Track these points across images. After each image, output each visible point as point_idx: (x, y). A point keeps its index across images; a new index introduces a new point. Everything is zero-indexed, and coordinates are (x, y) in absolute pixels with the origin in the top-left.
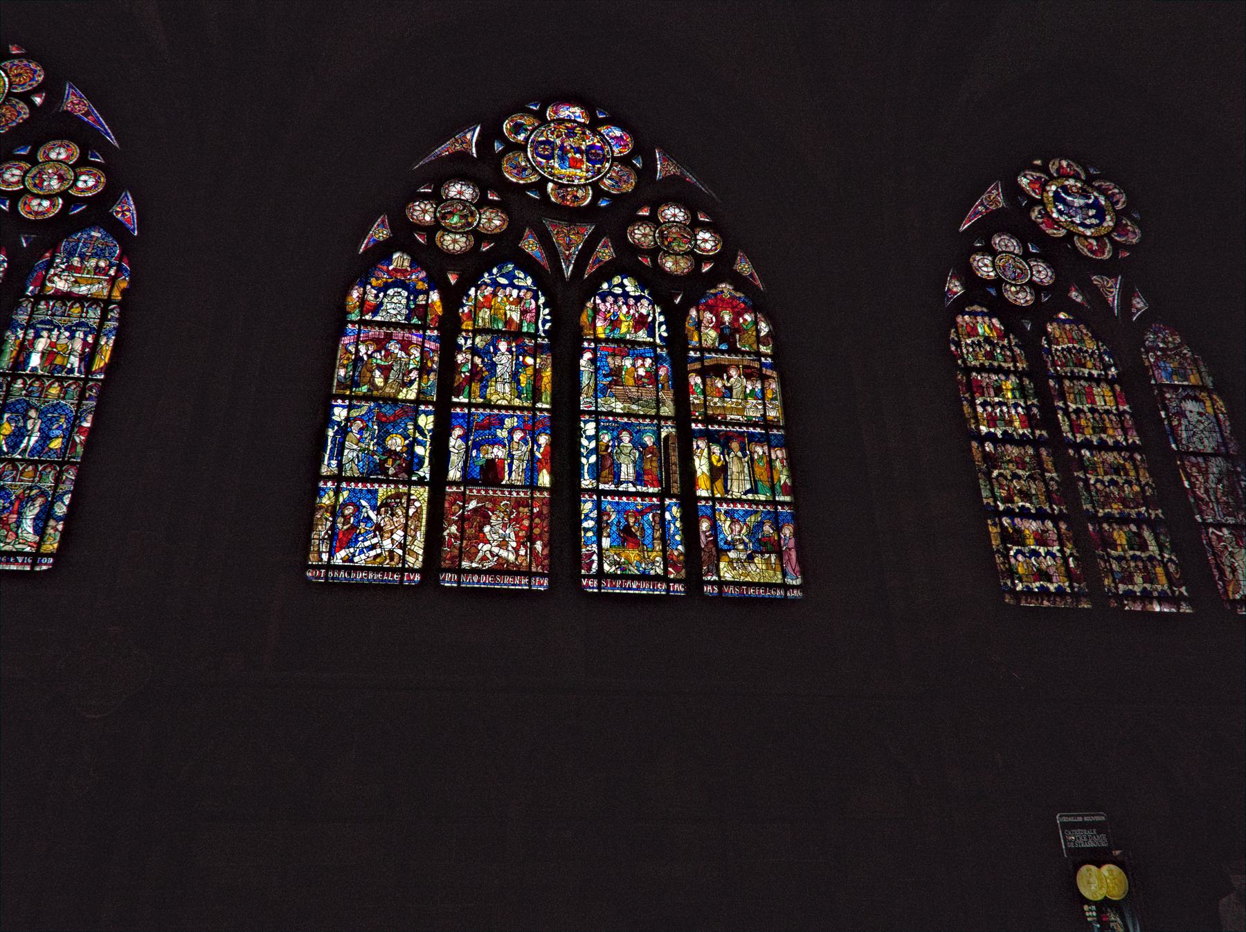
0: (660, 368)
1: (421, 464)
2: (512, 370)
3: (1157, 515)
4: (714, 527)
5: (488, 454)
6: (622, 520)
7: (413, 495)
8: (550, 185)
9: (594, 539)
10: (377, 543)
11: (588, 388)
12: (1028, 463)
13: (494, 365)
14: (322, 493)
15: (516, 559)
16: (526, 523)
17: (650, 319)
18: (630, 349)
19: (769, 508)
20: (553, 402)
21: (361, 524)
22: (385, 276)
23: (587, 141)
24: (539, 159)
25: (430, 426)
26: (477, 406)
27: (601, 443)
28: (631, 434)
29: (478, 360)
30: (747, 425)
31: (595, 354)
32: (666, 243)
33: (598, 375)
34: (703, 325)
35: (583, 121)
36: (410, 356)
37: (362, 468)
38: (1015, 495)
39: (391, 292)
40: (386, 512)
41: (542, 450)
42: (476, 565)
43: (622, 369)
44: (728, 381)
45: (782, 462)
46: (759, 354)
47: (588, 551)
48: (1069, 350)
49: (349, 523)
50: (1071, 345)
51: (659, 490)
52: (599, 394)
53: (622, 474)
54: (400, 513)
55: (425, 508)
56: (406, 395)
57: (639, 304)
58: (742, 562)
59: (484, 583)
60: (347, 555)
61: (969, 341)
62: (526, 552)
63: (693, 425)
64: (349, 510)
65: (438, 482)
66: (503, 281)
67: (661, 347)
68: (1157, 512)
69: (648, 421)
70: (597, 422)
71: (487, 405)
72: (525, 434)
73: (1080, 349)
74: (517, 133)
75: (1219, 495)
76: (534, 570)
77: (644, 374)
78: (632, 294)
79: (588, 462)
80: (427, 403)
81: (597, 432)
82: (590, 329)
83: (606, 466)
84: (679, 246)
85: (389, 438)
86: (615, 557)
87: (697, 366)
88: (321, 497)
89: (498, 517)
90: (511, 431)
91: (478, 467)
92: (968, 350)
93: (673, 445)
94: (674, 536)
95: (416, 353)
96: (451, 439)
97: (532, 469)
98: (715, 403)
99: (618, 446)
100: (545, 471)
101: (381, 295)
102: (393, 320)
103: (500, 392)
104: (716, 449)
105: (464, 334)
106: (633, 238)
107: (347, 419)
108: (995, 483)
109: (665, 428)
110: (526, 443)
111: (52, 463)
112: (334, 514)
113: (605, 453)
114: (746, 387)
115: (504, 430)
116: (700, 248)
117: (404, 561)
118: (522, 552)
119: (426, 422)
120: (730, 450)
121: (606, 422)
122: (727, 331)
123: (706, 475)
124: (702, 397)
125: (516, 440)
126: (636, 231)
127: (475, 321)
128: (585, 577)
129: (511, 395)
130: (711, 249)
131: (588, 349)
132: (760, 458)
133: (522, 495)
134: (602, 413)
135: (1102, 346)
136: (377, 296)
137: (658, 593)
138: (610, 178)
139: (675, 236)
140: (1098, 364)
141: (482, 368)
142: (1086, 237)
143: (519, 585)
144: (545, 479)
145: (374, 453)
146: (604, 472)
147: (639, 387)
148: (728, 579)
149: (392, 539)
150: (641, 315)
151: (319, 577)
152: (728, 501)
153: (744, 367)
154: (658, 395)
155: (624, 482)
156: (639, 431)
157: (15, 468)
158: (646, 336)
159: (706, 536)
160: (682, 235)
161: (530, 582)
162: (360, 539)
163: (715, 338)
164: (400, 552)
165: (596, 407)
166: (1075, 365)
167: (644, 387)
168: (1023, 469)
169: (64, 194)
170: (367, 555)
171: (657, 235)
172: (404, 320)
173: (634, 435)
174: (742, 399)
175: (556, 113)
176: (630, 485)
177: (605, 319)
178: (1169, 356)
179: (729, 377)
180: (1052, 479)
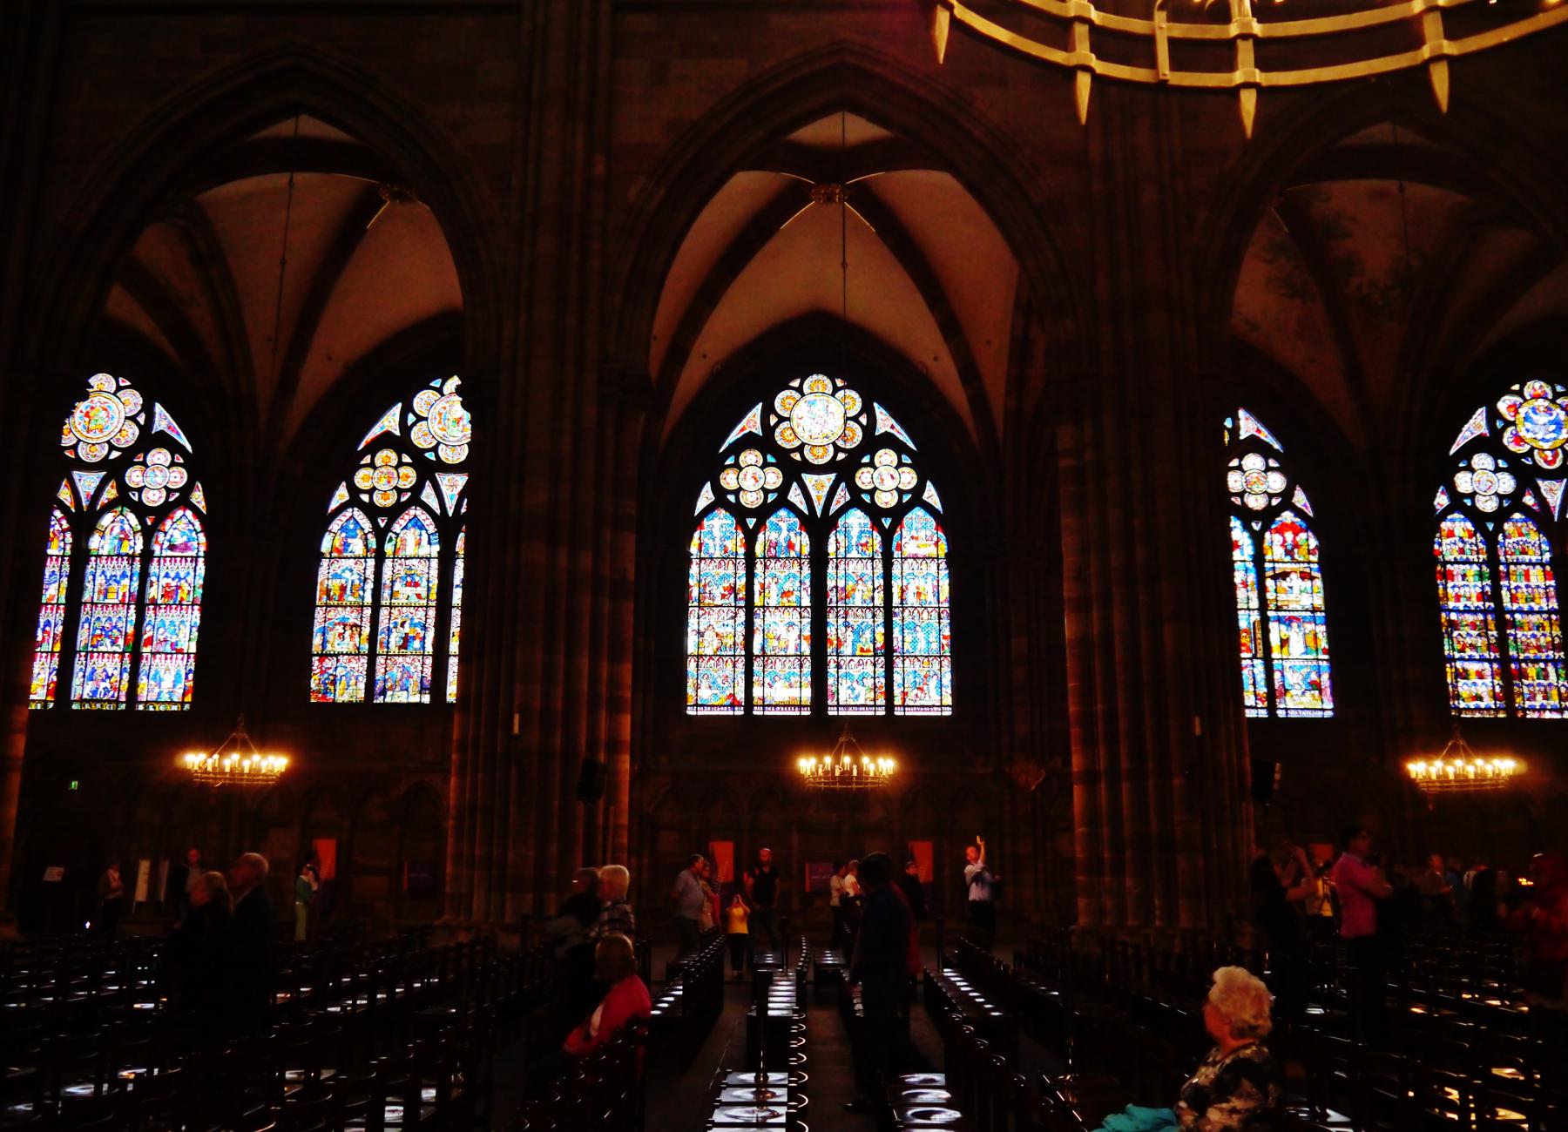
3: (1560, 656)
4: (1283, 676)
48: (1518, 543)
50: (1519, 539)
87: (1271, 573)
93: (1258, 626)
104: (1283, 627)
111: (935, 656)
122: (1289, 547)
139: (1255, 480)
142: (1543, 450)
153: (1301, 572)
157: (919, 661)
169: (897, 489)
180: (1493, 636)
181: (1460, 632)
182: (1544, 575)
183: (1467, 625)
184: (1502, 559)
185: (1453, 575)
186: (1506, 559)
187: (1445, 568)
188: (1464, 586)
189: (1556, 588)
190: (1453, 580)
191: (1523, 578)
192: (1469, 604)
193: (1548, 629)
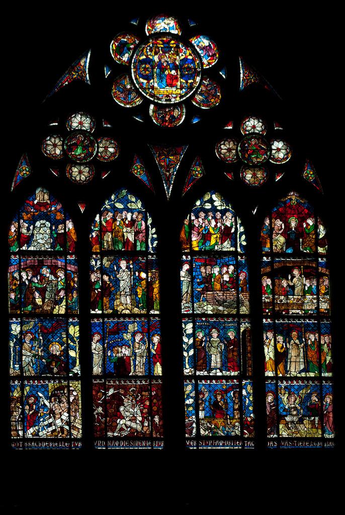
0: (241, 273)
1: (74, 365)
2: (131, 285)
4: (277, 399)
5: (118, 353)
6: (213, 397)
7: (71, 387)
8: (152, 107)
9: (194, 412)
10: (52, 422)
11: (187, 295)
13: (117, 282)
14: (13, 389)
15: (142, 429)
16: (147, 403)
17: (233, 230)
18: (217, 259)
19: (316, 382)
20: (160, 310)
21: (41, 409)
22: (32, 210)
23: (181, 54)
24: (141, 80)
25: (77, 335)
26: (109, 316)
27: (197, 339)
28: (219, 331)
29: (106, 278)
30: (304, 318)
31: (191, 266)
32: (247, 156)
33: (194, 284)
34: (274, 232)
35: (175, 32)
36: (58, 278)
37: (36, 369)
39: (38, 224)
40: (55, 400)
41: (156, 347)
42: (117, 434)
43: (212, 277)
44: (292, 280)
45: (328, 346)
46: (317, 255)
47: (190, 421)
49: (33, 409)
51: (238, 373)
52: (195, 300)
53: (212, 362)
54: (65, 401)
55: (80, 396)
56: (59, 310)
57: (224, 217)
58: (295, 424)
59: (123, 446)
60: (34, 431)
62: (149, 424)
63: (264, 320)
64: (31, 401)
65: (86, 375)
66: (119, 206)
67: (241, 255)
69: (230, 320)
70: (194, 323)
71: (116, 314)
72: (143, 336)
74: (122, 54)
76: (154, 436)
77: (228, 280)
78: (219, 208)
79: (188, 354)
80: (73, 317)
81: (194, 331)
82: (187, 244)
83: (201, 359)
84: (257, 158)
85: (51, 345)
86: (208, 424)
87: (268, 270)
88: (13, 392)
89: (129, 399)
90: (134, 334)
91: (113, 364)
94: (248, 406)
95: (61, 274)
96: (93, 344)
97: (150, 365)
98: (281, 301)
99: (209, 341)
100: (158, 363)
101: (31, 228)
102: (43, 249)
103: (124, 303)
104: (280, 338)
105: (94, 256)
106: (220, 153)
107: (21, 331)
109: (243, 324)
110: (144, 343)
112: (22, 404)
113: (200, 347)
114: (305, 285)
115: (128, 334)
116: (273, 159)
117: (69, 432)
118: (146, 424)
119: (74, 331)
120: (291, 339)
121: (201, 322)
122: (292, 237)
123: (272, 360)
124: (271, 296)
125: (137, 341)
126: (222, 146)
127: (101, 244)
128: (188, 439)
129: (132, 305)
130: (283, 158)
131: (186, 262)
132: (313, 343)
133: (144, 383)
134: (198, 315)
136: (28, 229)
137: (237, 448)
138: (201, 94)
141: (109, 284)
143: (145, 447)
144: (158, 370)
145: (42, 357)
146: (200, 362)
147: (224, 291)
148: (284, 436)
149: (62, 420)
150: (226, 227)
151: (19, 447)
152: (287, 379)
153: (305, 268)
154: (238, 297)
155: (214, 369)
156: (224, 327)
158: (229, 246)
159: (271, 406)
160: (260, 147)
161: (152, 444)
162: (41, 420)
163: (284, 243)
164: (67, 427)
165: (193, 310)
167: (228, 290)
170: (47, 430)
171: (239, 148)
172: (51, 248)
173: (221, 331)
174: (301, 296)
175: (153, 27)
176: (218, 371)
177: (199, 234)
179: (293, 277)
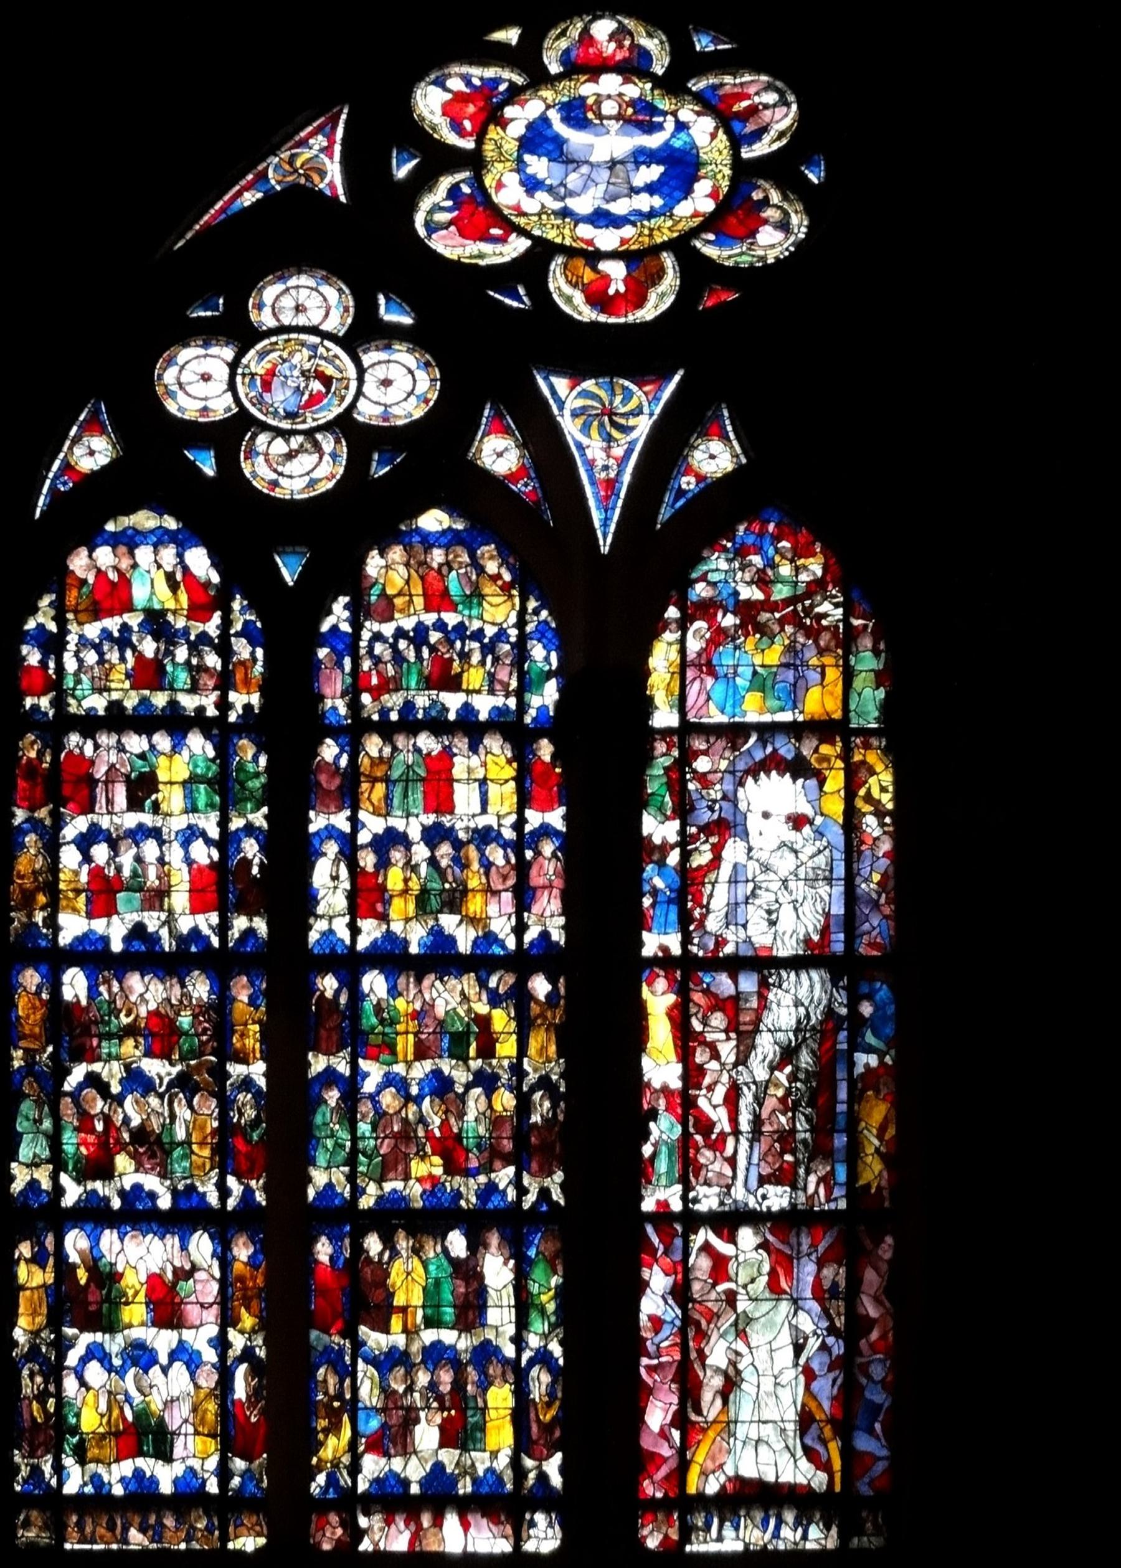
12: (186, 1034)
38: (122, 1147)
50: (430, 618)
61: (92, 631)
68: (547, 1182)
73: (461, 628)
75: (770, 1103)
92: (80, 661)
108: (67, 1107)
135: (536, 612)
140: (503, 674)
166: (430, 683)
168: (165, 1055)
178: (761, 629)
180: (247, 1083)
181: (97, 1067)
182: (519, 780)
183: (131, 1031)
184: (337, 705)
185: (93, 782)
186: (355, 706)
187: (57, 746)
188: (140, 834)
189: (569, 844)
190: (88, 807)
191: (417, 795)
192: (152, 921)
193: (507, 1048)
